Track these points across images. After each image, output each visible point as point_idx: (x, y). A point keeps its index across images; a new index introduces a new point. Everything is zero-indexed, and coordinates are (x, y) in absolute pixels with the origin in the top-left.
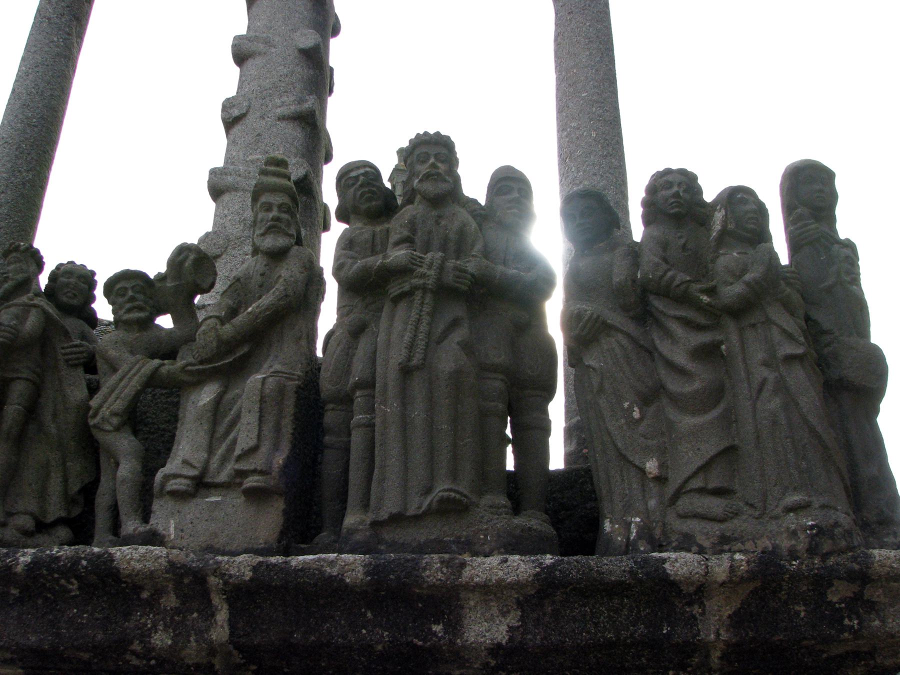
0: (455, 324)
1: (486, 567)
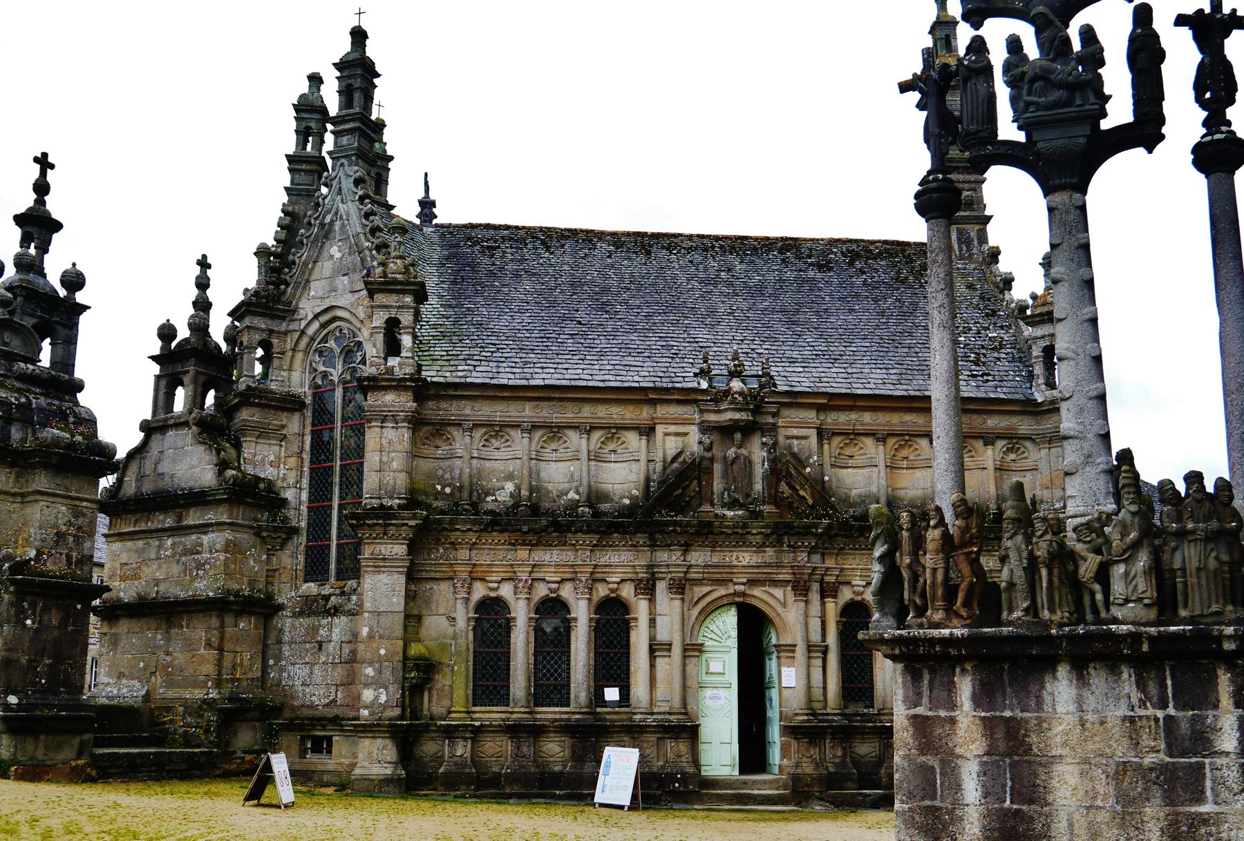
0: (1212, 550)
1: (1230, 630)
